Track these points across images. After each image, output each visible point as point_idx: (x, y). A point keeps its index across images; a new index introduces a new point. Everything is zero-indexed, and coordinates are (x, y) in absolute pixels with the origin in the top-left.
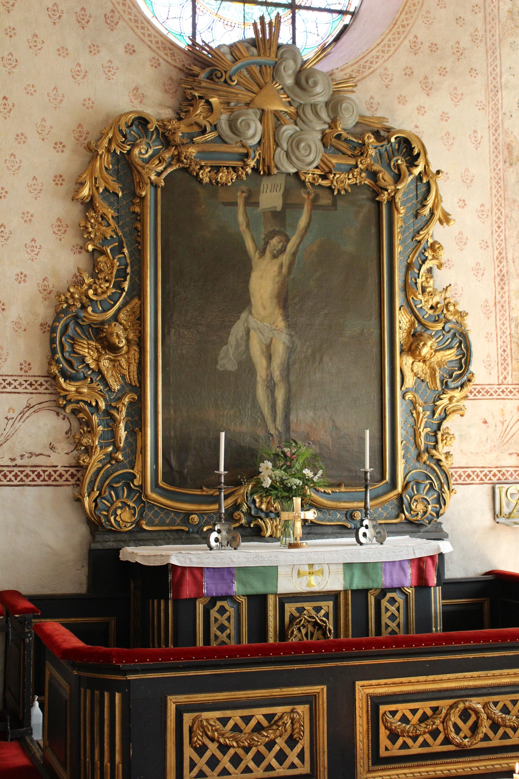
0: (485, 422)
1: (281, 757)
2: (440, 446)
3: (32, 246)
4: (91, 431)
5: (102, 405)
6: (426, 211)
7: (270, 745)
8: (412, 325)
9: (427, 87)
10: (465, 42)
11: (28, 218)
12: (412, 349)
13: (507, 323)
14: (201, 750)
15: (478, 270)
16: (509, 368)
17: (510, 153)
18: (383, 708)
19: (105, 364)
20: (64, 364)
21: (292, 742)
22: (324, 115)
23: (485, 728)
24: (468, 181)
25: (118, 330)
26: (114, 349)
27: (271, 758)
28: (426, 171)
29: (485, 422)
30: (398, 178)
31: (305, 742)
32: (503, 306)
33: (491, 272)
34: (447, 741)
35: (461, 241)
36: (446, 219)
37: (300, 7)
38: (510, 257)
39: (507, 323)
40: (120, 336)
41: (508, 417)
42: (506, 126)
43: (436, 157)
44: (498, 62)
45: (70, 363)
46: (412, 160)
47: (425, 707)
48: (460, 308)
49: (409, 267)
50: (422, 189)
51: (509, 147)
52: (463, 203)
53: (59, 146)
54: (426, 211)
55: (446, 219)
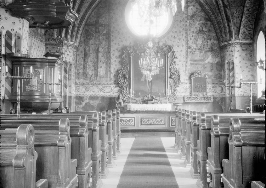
1: (131, 123)
3: (116, 66)
4: (124, 89)
5: (125, 85)
6: (173, 57)
7: (129, 122)
8: (171, 74)
9: (175, 38)
11: (115, 61)
12: (170, 77)
14: (121, 122)
18: (142, 119)
19: (125, 80)
20: (120, 80)
21: (132, 122)
22: (157, 44)
23: (155, 122)
25: (127, 76)
26: (126, 78)
27: (129, 123)
28: (173, 51)
30: (169, 52)
31: (133, 122)
34: (150, 123)
36: (177, 58)
40: (127, 76)
43: (175, 49)
45: (121, 80)
46: (171, 50)
47: (148, 119)
48: (179, 71)
49: (170, 65)
50: (173, 53)
53: (119, 51)
54: (173, 57)
55: (177, 58)
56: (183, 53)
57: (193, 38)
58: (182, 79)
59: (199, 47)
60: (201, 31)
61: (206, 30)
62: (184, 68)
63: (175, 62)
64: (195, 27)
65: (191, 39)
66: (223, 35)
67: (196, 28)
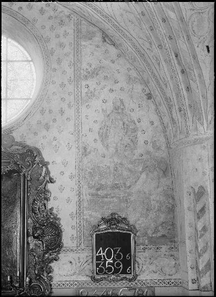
0: (71, 262)
2: (45, 274)
10: (65, 106)
13: (82, 221)
15: (69, 201)
16: (83, 240)
17: (85, 151)
24: (65, 164)
29: (71, 262)
32: (80, 214)
33: (75, 199)
35: (61, 189)
36: (51, 181)
37: (8, 99)
38: (84, 193)
39: (82, 221)
41: (81, 260)
42: (83, 140)
43: (47, 156)
44: (80, 114)
51: (85, 149)
52: (62, 173)
55: (51, 181)
56: (71, 170)
57: (96, 127)
58: (67, 239)
59: (112, 149)
60: (119, 108)
61: (132, 106)
62: (72, 208)
63: (46, 191)
64: (101, 99)
65: (90, 130)
66: (176, 115)
67: (104, 101)
